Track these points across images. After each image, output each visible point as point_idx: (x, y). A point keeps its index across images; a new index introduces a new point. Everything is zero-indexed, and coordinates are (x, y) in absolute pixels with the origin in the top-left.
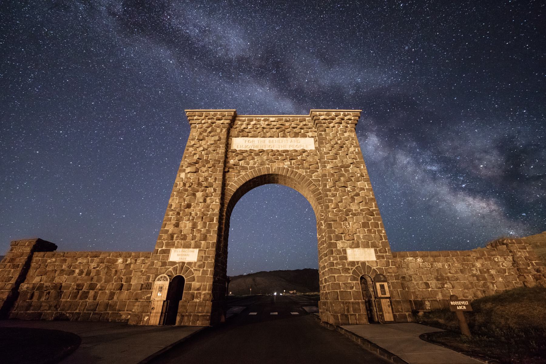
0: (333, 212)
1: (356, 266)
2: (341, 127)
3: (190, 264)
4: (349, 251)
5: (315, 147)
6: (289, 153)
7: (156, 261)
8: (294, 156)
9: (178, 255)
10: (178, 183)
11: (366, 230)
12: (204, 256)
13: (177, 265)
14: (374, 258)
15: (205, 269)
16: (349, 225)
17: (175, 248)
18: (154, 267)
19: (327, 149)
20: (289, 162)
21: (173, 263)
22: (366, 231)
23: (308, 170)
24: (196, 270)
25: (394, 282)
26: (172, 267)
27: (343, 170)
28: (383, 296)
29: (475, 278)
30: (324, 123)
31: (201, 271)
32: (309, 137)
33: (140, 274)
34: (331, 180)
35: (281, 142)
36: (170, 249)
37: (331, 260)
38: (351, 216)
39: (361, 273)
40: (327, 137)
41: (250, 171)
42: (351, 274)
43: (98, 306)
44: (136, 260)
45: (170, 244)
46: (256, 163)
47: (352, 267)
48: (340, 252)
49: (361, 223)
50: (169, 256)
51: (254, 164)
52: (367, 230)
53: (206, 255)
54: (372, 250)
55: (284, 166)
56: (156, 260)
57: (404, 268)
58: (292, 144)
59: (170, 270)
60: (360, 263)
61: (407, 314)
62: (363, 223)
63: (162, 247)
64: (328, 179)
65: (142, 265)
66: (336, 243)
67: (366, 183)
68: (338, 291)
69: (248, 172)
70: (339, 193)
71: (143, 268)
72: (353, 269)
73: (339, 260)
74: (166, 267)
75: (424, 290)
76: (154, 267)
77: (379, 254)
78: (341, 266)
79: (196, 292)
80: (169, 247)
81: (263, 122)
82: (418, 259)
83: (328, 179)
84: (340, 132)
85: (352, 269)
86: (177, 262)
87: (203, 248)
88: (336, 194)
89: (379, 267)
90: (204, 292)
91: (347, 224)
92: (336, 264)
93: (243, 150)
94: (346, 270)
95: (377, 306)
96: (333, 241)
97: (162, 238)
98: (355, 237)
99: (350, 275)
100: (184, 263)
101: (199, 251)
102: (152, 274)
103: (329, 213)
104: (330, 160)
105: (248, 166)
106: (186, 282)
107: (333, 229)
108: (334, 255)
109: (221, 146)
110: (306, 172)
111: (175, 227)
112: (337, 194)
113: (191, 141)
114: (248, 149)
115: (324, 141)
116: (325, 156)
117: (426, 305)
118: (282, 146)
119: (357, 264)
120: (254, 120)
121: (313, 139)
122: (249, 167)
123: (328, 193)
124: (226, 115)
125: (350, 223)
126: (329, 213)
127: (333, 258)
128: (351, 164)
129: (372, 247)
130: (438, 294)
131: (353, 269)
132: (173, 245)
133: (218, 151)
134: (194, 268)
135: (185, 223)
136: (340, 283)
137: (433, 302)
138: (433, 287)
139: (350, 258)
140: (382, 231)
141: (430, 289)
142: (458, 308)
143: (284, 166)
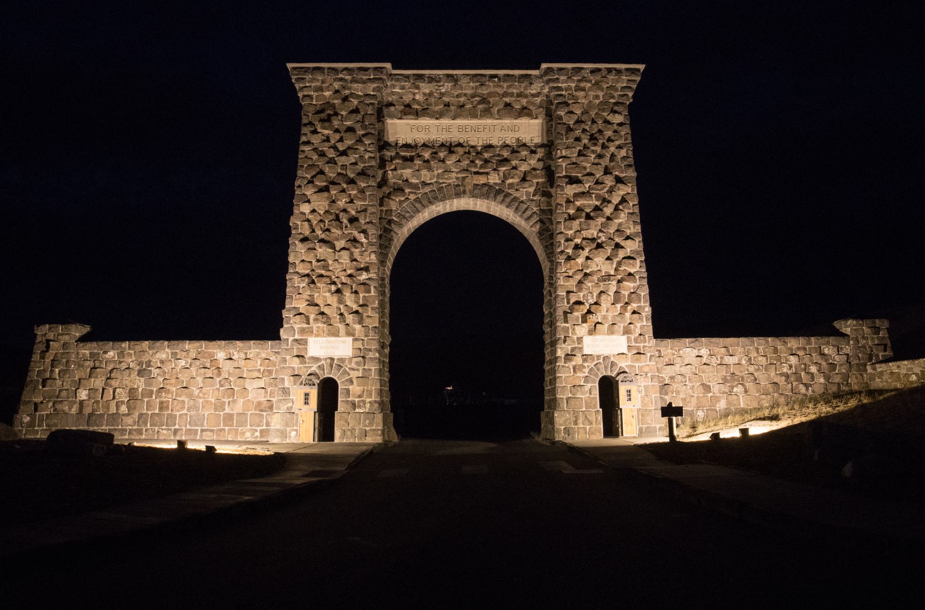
3: (342, 360)
9: (321, 348)
17: (315, 337)
20: (497, 175)
21: (317, 359)
25: (649, 385)
29: (783, 378)
31: (360, 371)
36: (307, 339)
43: (206, 421)
45: (306, 331)
47: (589, 364)
50: (306, 348)
60: (602, 359)
61: (658, 426)
63: (294, 336)
71: (260, 366)
75: (700, 395)
80: (305, 335)
85: (588, 367)
86: (322, 358)
90: (368, 400)
91: (589, 298)
100: (332, 359)
119: (598, 359)
130: (720, 401)
131: (590, 367)
134: (349, 366)
135: (323, 296)
137: (710, 412)
138: (715, 392)
139: (586, 351)
140: (644, 309)
141: (710, 395)
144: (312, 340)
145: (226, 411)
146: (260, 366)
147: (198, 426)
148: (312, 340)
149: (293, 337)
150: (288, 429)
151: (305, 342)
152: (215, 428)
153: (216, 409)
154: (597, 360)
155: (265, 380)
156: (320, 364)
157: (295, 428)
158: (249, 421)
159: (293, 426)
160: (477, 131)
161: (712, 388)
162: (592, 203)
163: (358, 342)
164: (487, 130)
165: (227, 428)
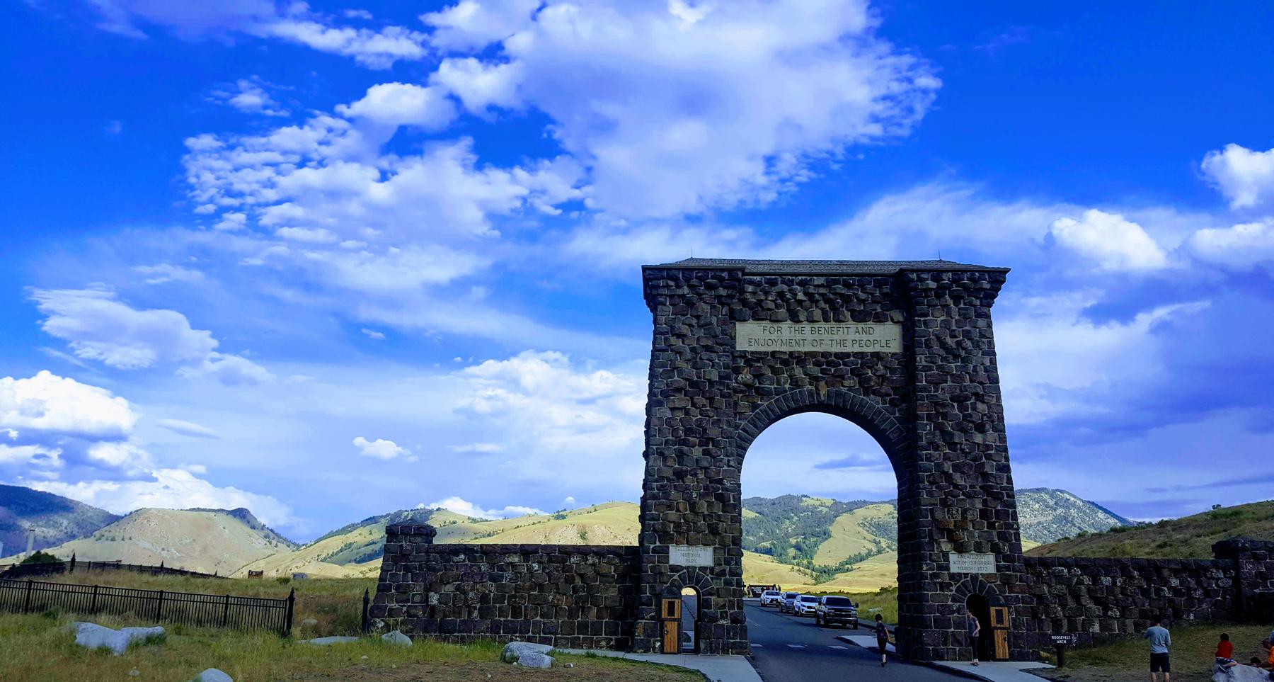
1: (962, 581)
2: (962, 306)
3: (703, 569)
4: (953, 557)
5: (904, 345)
6: (852, 358)
13: (685, 571)
14: (991, 569)
15: (728, 576)
18: (650, 573)
19: (928, 359)
21: (675, 569)
23: (888, 398)
24: (717, 579)
28: (999, 625)
30: (927, 296)
32: (892, 320)
33: (611, 580)
34: (931, 427)
35: (835, 332)
38: (962, 497)
39: (970, 592)
41: (777, 397)
42: (954, 592)
48: (939, 558)
50: (668, 556)
51: (785, 383)
56: (651, 563)
57: (1046, 583)
58: (857, 337)
59: (675, 578)
64: (927, 424)
68: (932, 615)
69: (773, 400)
70: (944, 454)
71: (614, 572)
83: (927, 424)
84: (957, 318)
88: (938, 456)
89: (999, 582)
90: (731, 611)
92: (931, 575)
93: (760, 353)
98: (966, 533)
99: (952, 593)
102: (648, 583)
103: (924, 491)
105: (772, 387)
107: (929, 518)
110: (884, 402)
114: (770, 349)
116: (924, 374)
118: (838, 341)
120: (779, 282)
124: (727, 277)
127: (927, 566)
128: (973, 394)
129: (991, 551)
132: (672, 540)
133: (717, 361)
134: (712, 576)
144: (673, 549)
145: (580, 619)
146: (614, 572)
147: (552, 633)
148: (673, 549)
150: (652, 640)
151: (666, 551)
153: (570, 617)
157: (659, 638)
159: (657, 637)
163: (718, 551)
164: (840, 333)
165: (581, 636)
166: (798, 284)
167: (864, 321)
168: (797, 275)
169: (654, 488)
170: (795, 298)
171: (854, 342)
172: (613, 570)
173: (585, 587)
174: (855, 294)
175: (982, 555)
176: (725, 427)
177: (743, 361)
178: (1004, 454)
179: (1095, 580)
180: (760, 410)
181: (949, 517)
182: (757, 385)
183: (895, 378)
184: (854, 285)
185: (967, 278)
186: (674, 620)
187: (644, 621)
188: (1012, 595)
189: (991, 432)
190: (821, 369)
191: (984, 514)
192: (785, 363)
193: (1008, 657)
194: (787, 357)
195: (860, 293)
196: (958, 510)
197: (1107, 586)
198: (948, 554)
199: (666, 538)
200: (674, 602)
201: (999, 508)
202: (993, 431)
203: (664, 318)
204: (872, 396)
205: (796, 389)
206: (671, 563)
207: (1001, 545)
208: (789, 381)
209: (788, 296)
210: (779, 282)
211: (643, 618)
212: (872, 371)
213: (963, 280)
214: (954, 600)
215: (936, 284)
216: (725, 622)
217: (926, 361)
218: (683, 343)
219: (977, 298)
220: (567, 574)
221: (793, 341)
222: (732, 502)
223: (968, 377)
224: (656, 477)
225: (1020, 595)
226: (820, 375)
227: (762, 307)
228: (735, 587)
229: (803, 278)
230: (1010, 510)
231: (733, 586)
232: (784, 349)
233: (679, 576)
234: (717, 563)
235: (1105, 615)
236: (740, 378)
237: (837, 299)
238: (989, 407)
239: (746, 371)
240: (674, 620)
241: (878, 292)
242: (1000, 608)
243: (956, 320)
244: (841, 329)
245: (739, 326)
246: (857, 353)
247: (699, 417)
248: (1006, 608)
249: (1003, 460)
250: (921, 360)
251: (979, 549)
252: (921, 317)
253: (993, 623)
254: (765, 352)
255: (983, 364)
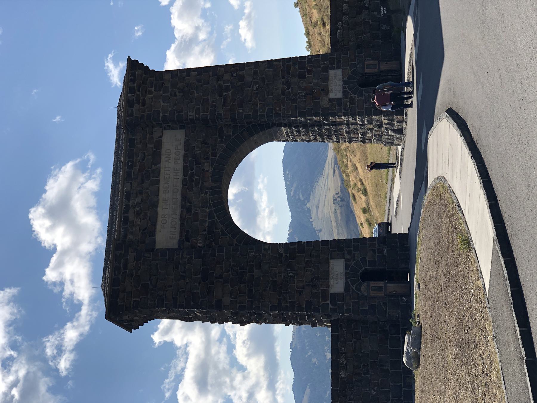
0: (285, 109)
1: (348, 90)
2: (153, 89)
3: (347, 267)
4: (332, 95)
5: (181, 128)
6: (188, 164)
7: (345, 306)
8: (193, 158)
10: (238, 305)
11: (307, 75)
12: (337, 252)
14: (339, 72)
16: (302, 92)
17: (329, 287)
18: (351, 308)
20: (205, 164)
21: (347, 287)
22: (309, 75)
23: (219, 140)
26: (352, 285)
27: (226, 93)
28: (377, 67)
31: (355, 252)
32: (161, 137)
34: (240, 109)
35: (168, 176)
36: (331, 294)
37: (341, 114)
38: (290, 90)
40: (170, 109)
42: (356, 96)
44: (342, 353)
46: (203, 210)
47: (349, 94)
49: (299, 80)
51: (205, 212)
52: (308, 74)
53: (337, 250)
54: (332, 72)
55: (210, 171)
57: (348, 43)
59: (354, 288)
60: (345, 86)
62: (299, 78)
63: (329, 303)
64: (238, 112)
65: (347, 344)
66: (322, 109)
67: (246, 68)
68: (373, 109)
69: (218, 221)
70: (260, 101)
71: (351, 341)
72: (351, 93)
73: (342, 107)
74: (351, 293)
76: (351, 308)
77: (335, 65)
78: (348, 104)
79: (377, 254)
81: (132, 201)
82: (339, 27)
83: (238, 112)
84: (161, 92)
87: (329, 254)
89: (348, 68)
90: (377, 246)
92: (345, 110)
94: (352, 101)
95: (387, 75)
96: (320, 111)
97: (317, 307)
100: (346, 273)
101: (332, 258)
104: (210, 108)
106: (367, 266)
107: (306, 111)
108: (336, 111)
109: (176, 257)
111: (303, 293)
112: (260, 103)
113: (165, 302)
114: (178, 223)
115: (176, 114)
116: (201, 114)
117: (386, 29)
120: (126, 215)
121: (164, 131)
122: (209, 219)
123: (259, 114)
124: (120, 252)
125: (299, 91)
126: (286, 114)
131: (351, 93)
136: (365, 107)
139: (340, 95)
142: (385, 13)
143: (210, 171)
144: (332, 290)
145: (389, 368)
146: (351, 341)
148: (332, 290)
149: (329, 305)
150: (401, 304)
151: (334, 295)
152: (403, 376)
154: (347, 89)
155: (363, 337)
156: (350, 283)
157: (400, 298)
158: (396, 348)
160: (169, 180)
161: (366, 21)
162: (231, 94)
166: (129, 201)
167: (160, 155)
168: (122, 202)
169: (286, 306)
170: (140, 203)
171: (176, 162)
172: (350, 342)
173: (364, 365)
174: (139, 161)
175: (329, 78)
176: (239, 253)
177: (186, 243)
178: (260, 64)
179: (345, 14)
180: (226, 230)
181: (304, 98)
182: (206, 232)
183: (204, 135)
184: (132, 162)
185: (133, 84)
186: (385, 286)
187: (387, 311)
188: (356, 60)
189: (245, 71)
190: (196, 186)
191: (302, 76)
192: (189, 210)
193: (399, 62)
194: (185, 210)
195: (139, 158)
196: (299, 92)
197: (349, 7)
198: (330, 99)
199: (325, 294)
200: (372, 287)
201: (297, 67)
202: (244, 70)
203: (149, 302)
204: (216, 150)
205: (210, 204)
206: (344, 292)
207: (323, 66)
208: (204, 209)
209: (138, 209)
210: (126, 215)
211: (386, 311)
212: (198, 150)
213: (134, 87)
214: (362, 95)
215: (135, 105)
216: (385, 250)
217: (193, 112)
218: (171, 286)
219: (147, 79)
220: (354, 379)
221: (173, 206)
222: (296, 246)
223: (205, 86)
224: (277, 305)
225: (356, 55)
226: (200, 187)
227: (146, 229)
228: (359, 243)
229: (124, 197)
230: (299, 60)
231: (359, 244)
232: (178, 212)
233: (353, 284)
234: (342, 257)
235: (368, 8)
236: (200, 245)
237: (142, 174)
238: (226, 72)
239: (194, 240)
240: (385, 286)
241: (139, 146)
242: (366, 66)
243: (163, 93)
244: (166, 172)
245: (158, 246)
246: (185, 161)
247: (230, 273)
248: (366, 62)
249: (264, 64)
250: (191, 115)
251: (326, 79)
252: (160, 115)
253: (376, 70)
254: (181, 226)
255: (196, 76)
